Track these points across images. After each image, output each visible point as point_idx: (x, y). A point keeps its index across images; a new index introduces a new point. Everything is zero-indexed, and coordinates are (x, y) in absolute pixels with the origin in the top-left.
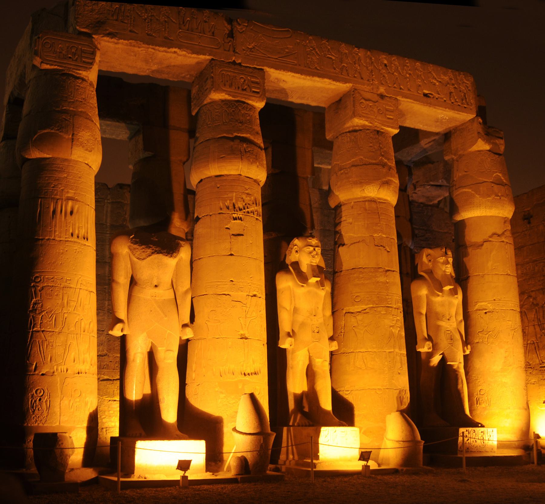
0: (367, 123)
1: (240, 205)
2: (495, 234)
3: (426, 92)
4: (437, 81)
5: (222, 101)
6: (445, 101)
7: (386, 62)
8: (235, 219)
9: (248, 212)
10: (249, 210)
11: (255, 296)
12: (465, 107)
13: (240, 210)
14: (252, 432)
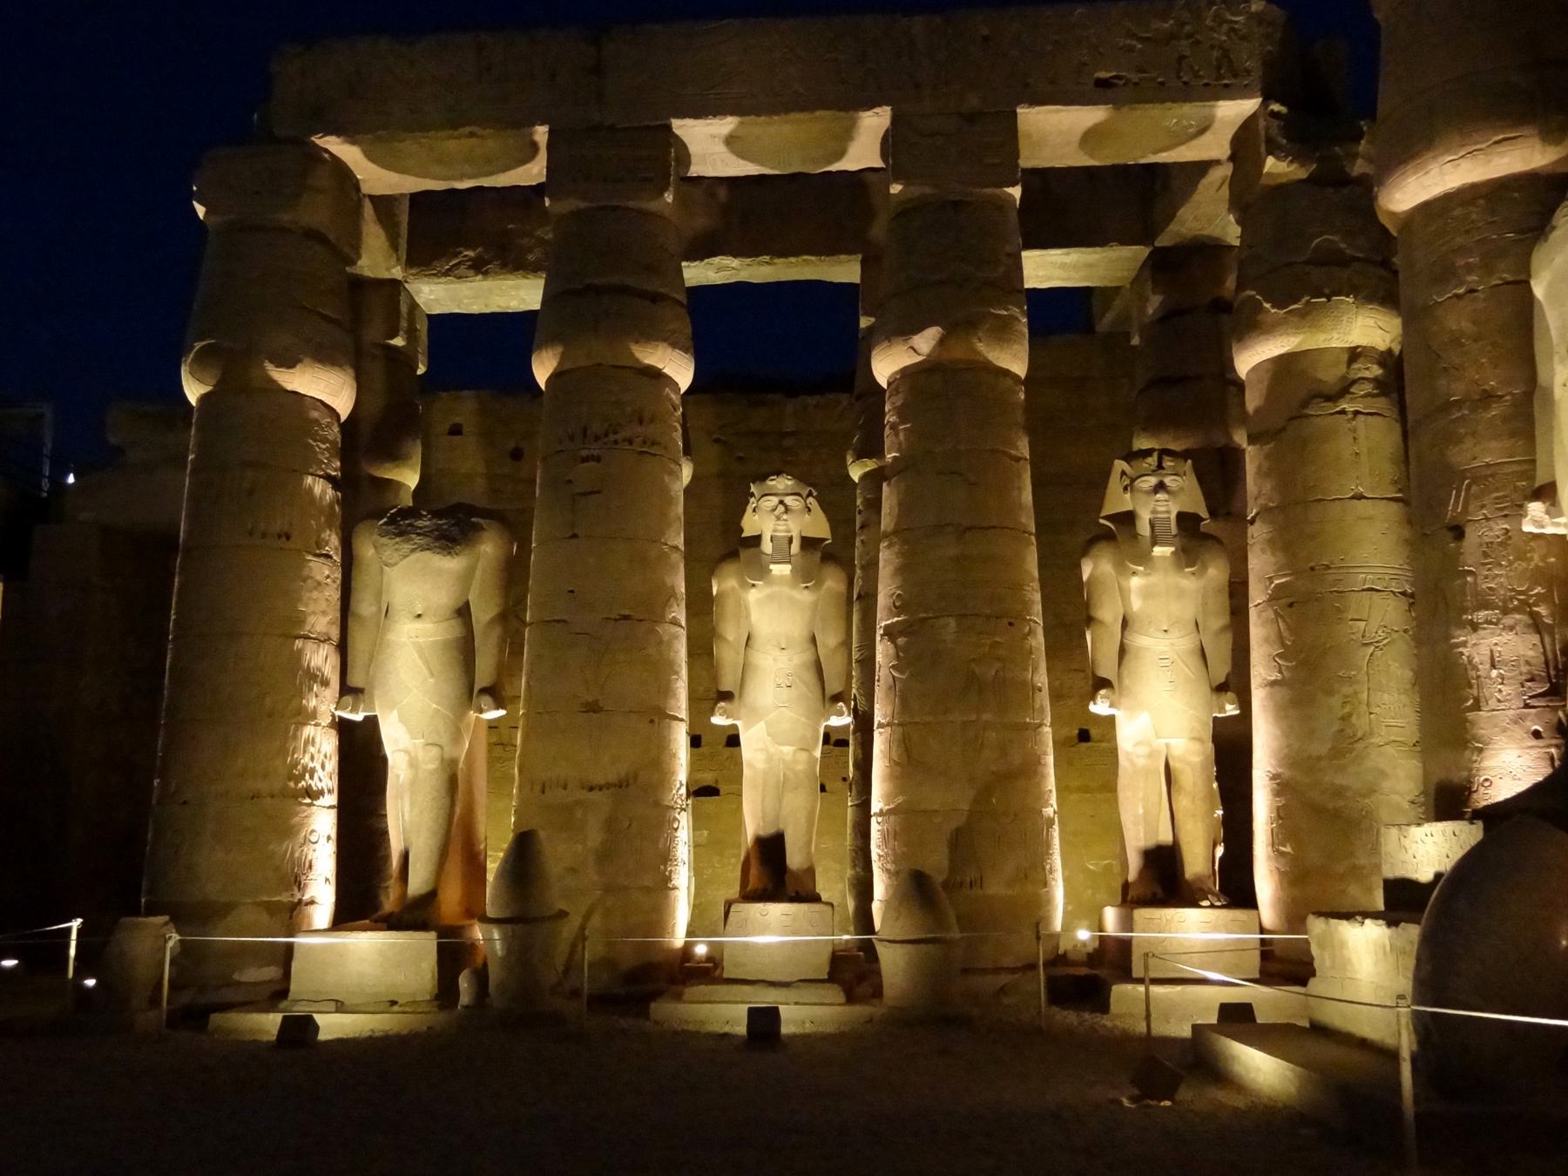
0: (928, 190)
1: (596, 427)
2: (1315, 396)
3: (1103, 75)
4: (1140, 39)
5: (572, 213)
6: (1162, 84)
7: (985, 32)
8: (585, 460)
9: (616, 442)
10: (619, 437)
11: (626, 618)
12: (1226, 86)
13: (597, 438)
14: (500, 916)
